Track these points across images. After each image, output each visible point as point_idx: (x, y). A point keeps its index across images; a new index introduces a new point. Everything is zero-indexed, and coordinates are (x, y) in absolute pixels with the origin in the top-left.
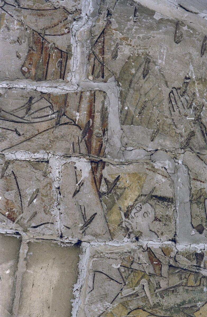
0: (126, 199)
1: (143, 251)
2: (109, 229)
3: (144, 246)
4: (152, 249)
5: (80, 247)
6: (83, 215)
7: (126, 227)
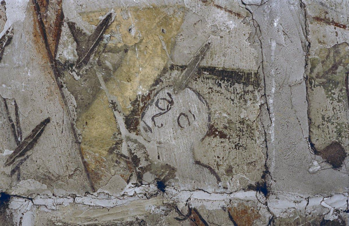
0: (129, 80)
1: (177, 219)
2: (84, 163)
3: (181, 206)
4: (201, 213)
5: (5, 212)
6: (13, 125)
7: (131, 153)
